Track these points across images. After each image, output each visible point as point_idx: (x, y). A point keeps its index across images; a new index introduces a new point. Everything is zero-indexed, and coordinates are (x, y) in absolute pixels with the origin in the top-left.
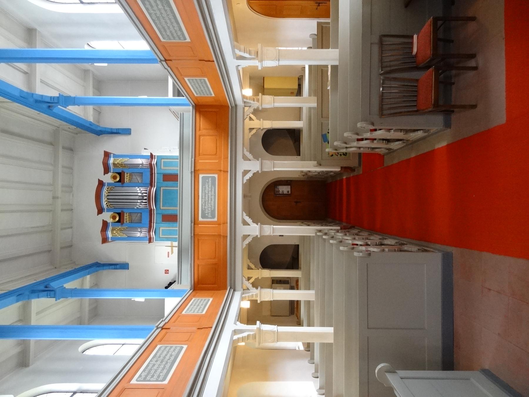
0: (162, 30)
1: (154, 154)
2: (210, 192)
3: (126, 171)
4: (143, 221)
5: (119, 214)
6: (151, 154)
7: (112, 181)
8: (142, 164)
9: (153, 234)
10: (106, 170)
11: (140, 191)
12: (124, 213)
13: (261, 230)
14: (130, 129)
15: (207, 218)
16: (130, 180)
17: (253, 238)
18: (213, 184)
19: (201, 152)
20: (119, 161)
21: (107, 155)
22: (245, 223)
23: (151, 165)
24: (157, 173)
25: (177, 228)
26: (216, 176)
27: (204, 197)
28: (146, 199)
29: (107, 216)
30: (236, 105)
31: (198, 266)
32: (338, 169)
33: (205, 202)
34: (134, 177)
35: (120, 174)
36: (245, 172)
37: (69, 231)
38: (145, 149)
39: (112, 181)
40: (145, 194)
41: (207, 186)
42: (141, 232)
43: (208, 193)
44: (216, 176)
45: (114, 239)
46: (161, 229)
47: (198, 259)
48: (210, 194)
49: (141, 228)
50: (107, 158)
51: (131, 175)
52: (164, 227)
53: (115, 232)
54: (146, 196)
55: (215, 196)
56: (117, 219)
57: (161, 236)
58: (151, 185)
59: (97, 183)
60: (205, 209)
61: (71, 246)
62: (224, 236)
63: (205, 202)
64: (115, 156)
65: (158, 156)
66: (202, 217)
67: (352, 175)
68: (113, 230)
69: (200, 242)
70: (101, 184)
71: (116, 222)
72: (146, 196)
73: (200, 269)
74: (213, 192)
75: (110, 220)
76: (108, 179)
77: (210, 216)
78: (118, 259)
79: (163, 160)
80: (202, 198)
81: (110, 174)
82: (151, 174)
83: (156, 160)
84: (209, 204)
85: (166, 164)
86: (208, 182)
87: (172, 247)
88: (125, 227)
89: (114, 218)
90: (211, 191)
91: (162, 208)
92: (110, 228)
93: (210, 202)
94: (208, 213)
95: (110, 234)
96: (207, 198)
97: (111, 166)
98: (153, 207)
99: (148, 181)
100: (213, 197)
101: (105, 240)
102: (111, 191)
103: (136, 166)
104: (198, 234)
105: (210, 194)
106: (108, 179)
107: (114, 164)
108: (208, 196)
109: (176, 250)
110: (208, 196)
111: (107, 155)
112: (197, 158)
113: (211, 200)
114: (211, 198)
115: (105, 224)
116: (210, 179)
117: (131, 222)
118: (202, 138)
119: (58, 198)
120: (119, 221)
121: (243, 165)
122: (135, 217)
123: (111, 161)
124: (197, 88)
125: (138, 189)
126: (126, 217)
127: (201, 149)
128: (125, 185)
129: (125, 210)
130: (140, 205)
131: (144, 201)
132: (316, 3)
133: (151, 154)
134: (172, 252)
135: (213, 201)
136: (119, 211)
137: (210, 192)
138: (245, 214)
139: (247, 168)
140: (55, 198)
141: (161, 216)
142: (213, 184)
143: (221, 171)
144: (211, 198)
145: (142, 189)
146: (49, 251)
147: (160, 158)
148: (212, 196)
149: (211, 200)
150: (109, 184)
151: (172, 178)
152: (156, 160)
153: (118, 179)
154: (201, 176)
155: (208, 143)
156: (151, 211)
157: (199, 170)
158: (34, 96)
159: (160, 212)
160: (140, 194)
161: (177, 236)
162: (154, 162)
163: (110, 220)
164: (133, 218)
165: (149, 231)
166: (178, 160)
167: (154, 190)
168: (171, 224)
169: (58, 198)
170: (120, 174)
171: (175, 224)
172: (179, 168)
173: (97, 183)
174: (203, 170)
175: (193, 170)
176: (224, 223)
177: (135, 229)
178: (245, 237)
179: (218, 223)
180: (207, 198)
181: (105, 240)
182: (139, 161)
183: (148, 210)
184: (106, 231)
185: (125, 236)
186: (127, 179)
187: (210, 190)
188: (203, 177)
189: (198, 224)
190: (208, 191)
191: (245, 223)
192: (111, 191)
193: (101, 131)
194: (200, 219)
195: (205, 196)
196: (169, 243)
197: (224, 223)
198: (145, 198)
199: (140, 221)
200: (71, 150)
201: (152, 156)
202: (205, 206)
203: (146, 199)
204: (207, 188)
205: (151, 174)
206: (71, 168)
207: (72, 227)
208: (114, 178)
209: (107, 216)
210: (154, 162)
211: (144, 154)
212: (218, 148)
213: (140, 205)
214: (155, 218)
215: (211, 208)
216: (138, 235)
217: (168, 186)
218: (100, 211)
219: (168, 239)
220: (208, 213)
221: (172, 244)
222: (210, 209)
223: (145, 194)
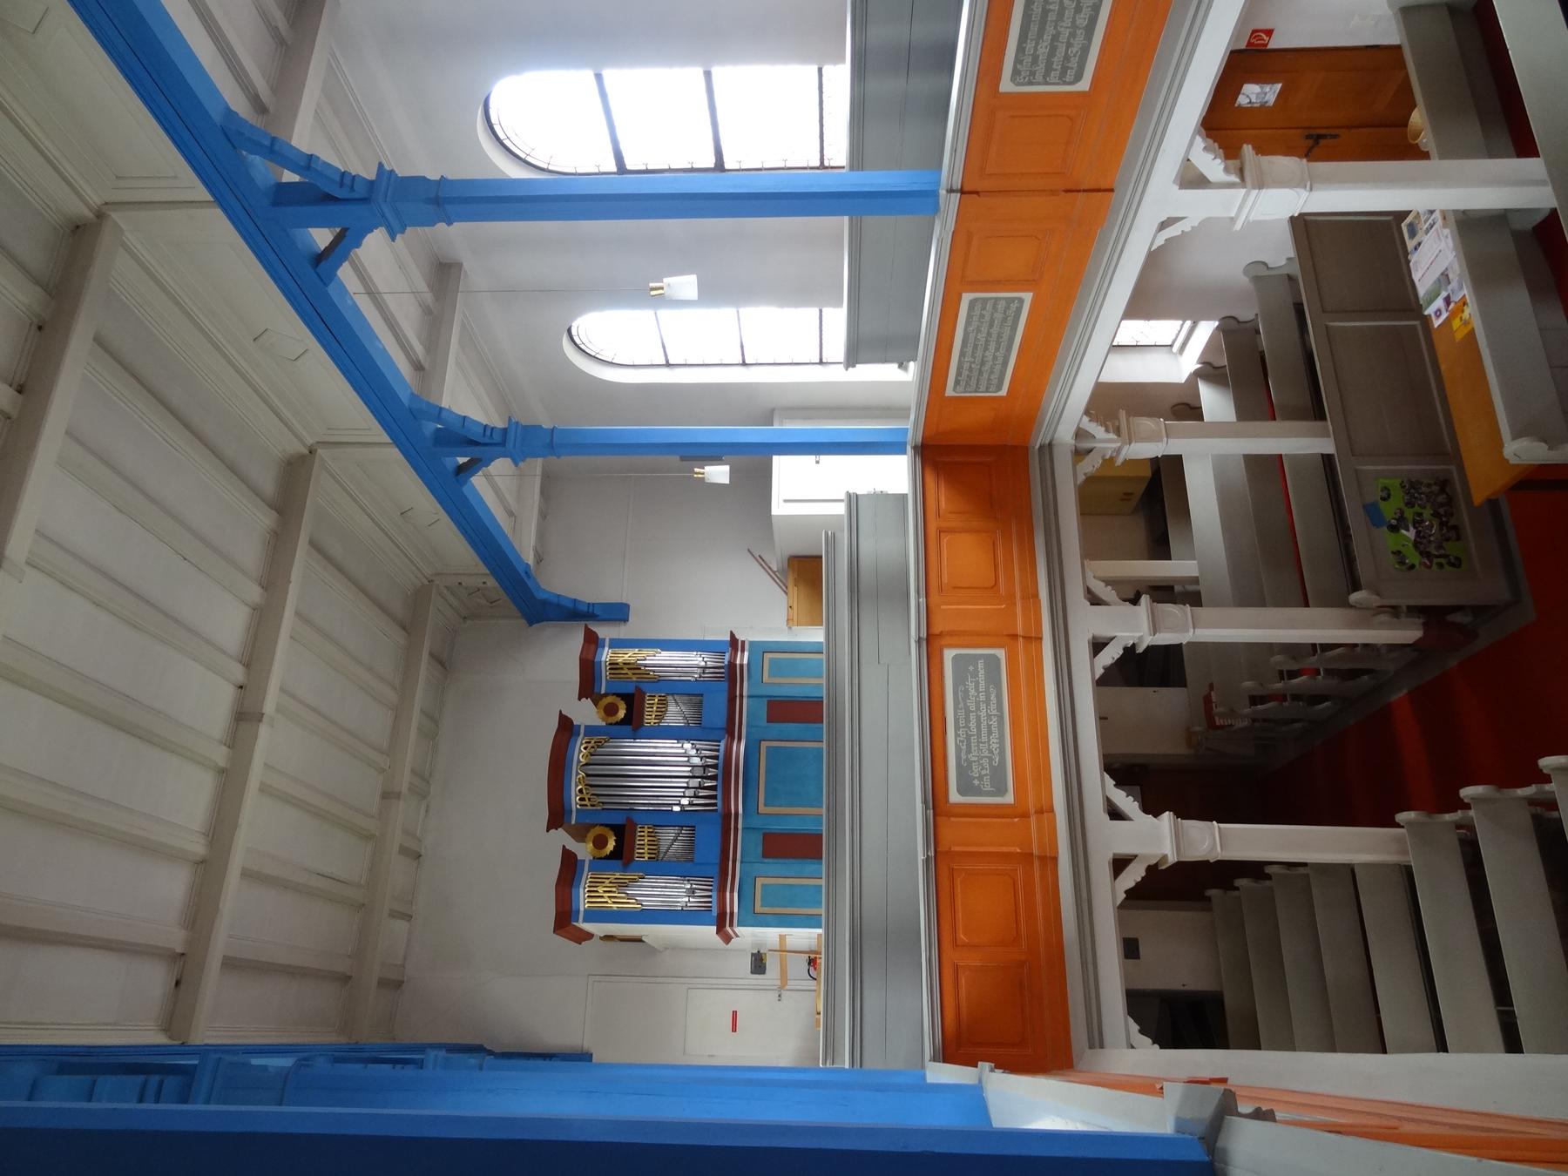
0: (1034, 28)
1: (740, 637)
2: (983, 706)
6: (732, 635)
9: (733, 901)
10: (588, 686)
12: (633, 826)
13: (1178, 836)
14: (627, 606)
15: (979, 793)
17: (1152, 870)
18: (993, 679)
19: (945, 579)
20: (628, 655)
22: (1115, 814)
23: (732, 665)
26: (1001, 653)
27: (962, 723)
28: (714, 778)
30: (1050, 445)
31: (956, 968)
32: (1408, 634)
33: (968, 737)
36: (1098, 646)
37: (400, 926)
41: (971, 686)
42: (692, 892)
43: (978, 708)
44: (1001, 653)
46: (760, 882)
47: (955, 944)
48: (983, 714)
52: (774, 877)
53: (601, 890)
54: (715, 766)
55: (1001, 718)
57: (758, 909)
58: (730, 730)
60: (970, 763)
61: (398, 985)
62: (1042, 859)
63: (968, 737)
65: (752, 643)
66: (961, 791)
67: (1453, 663)
68: (594, 884)
69: (958, 882)
70: (566, 727)
71: (607, 857)
72: (715, 766)
73: (963, 981)
74: (993, 707)
77: (988, 788)
78: (554, 1038)
80: (957, 728)
84: (984, 747)
85: (777, 668)
86: (975, 674)
90: (988, 702)
91: (762, 809)
92: (586, 877)
93: (984, 739)
94: (980, 778)
95: (583, 902)
96: (973, 725)
97: (605, 674)
99: (720, 720)
100: (994, 722)
104: (948, 852)
105: (983, 714)
107: (614, 666)
108: (978, 718)
110: (978, 718)
112: (935, 598)
113: (990, 733)
114: (989, 727)
115: (570, 866)
116: (981, 664)
117: (655, 857)
118: (945, 539)
119: (398, 796)
120: (615, 855)
121: (1087, 622)
123: (606, 655)
124: (975, 347)
125: (688, 746)
127: (945, 571)
131: (708, 784)
132: (1308, 137)
133: (732, 635)
135: (996, 734)
136: (619, 819)
137: (983, 706)
138: (1110, 782)
139: (1103, 632)
140: (388, 795)
142: (993, 679)
143: (1015, 637)
144: (989, 727)
145: (699, 745)
146: (345, 979)
147: (761, 649)
148: (989, 717)
149: (990, 733)
150: (591, 731)
151: (800, 711)
153: (622, 714)
154: (949, 654)
155: (968, 555)
156: (726, 816)
157: (940, 635)
158: (444, 415)
159: (756, 822)
160: (696, 761)
162: (743, 658)
163: (584, 851)
164: (664, 845)
165: (722, 890)
166: (823, 656)
168: (794, 866)
169: (398, 796)
171: (809, 866)
174: (952, 633)
175: (924, 634)
176: (1040, 812)
178: (1120, 864)
179: (1017, 813)
180: (973, 725)
181: (564, 921)
184: (571, 886)
187: (982, 698)
188: (955, 658)
189: (949, 815)
190: (978, 704)
191: (1115, 814)
193: (545, 603)
194: (955, 797)
195: (967, 720)
197: (1040, 812)
198: (712, 772)
200: (442, 663)
201: (734, 643)
202: (969, 751)
203: (714, 778)
204: (972, 692)
206: (435, 722)
207: (408, 917)
208: (610, 710)
210: (743, 658)
212: (1001, 567)
214: (743, 844)
215: (991, 759)
218: (557, 817)
220: (980, 778)
222: (985, 762)
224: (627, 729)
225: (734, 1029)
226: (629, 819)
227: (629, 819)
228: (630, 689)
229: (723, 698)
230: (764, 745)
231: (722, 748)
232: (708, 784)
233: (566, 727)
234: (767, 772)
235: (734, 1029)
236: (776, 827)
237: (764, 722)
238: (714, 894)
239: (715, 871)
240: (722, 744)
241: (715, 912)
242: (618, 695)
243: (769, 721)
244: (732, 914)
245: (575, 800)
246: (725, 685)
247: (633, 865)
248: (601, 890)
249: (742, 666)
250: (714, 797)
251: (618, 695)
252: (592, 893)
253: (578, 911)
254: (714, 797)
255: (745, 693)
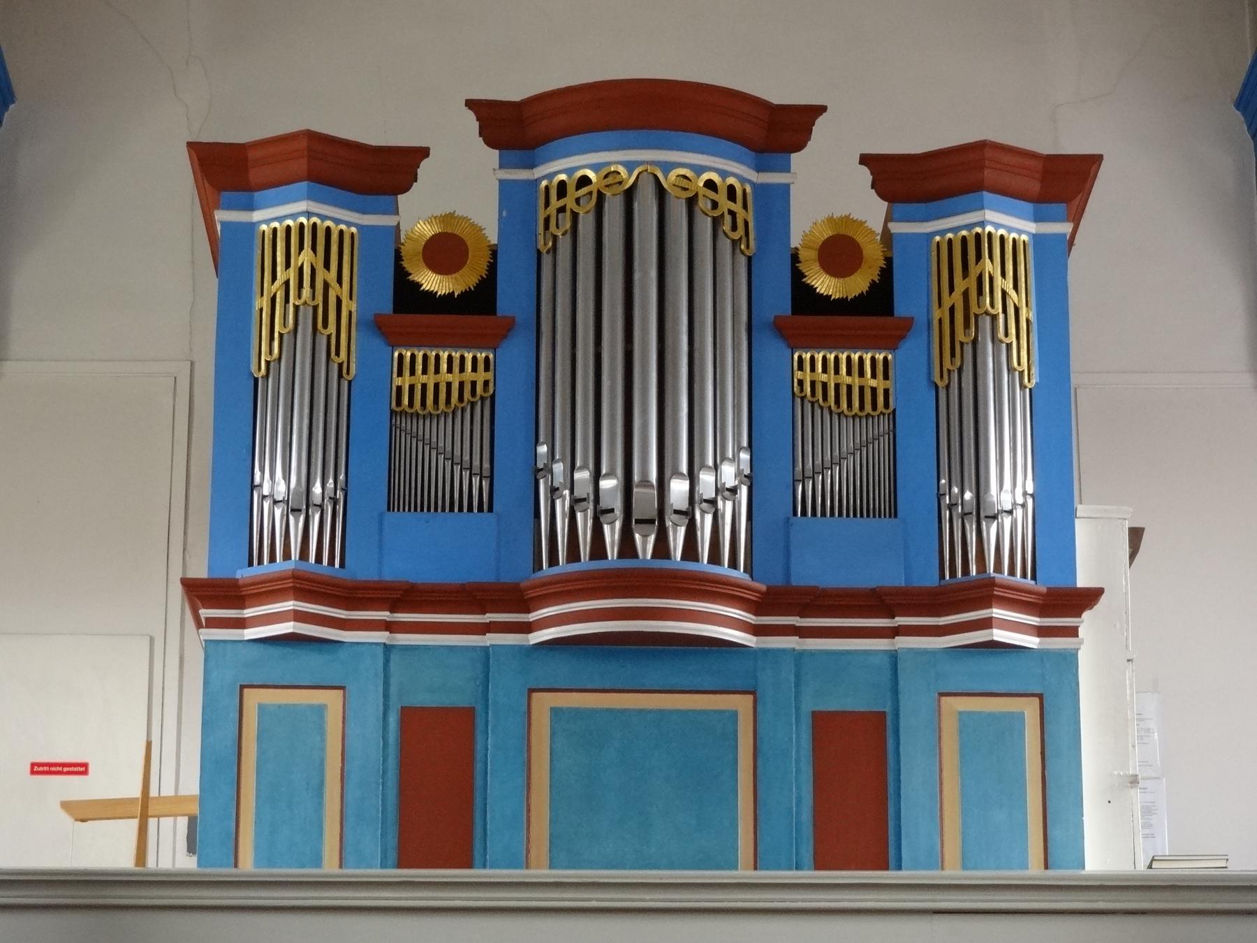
1: (1088, 622)
3: (911, 356)
4: (407, 523)
5: (480, 299)
6: (1091, 597)
7: (805, 224)
8: (981, 513)
9: (276, 619)
11: (716, 484)
12: (492, 340)
16: (818, 399)
20: (1010, 293)
21: (1062, 182)
23: (983, 593)
24: (894, 656)
25: (330, 867)
29: (461, 187)
34: (849, 435)
35: (879, 298)
38: (1136, 535)
39: (805, 224)
40: (677, 539)
42: (300, 505)
45: (230, 254)
46: (332, 700)
49: (342, 504)
50: (1035, 187)
51: (876, 408)
53: (306, 258)
54: (662, 549)
56: (431, 282)
57: (253, 698)
58: (777, 601)
59: (779, 90)
64: (1052, 258)
65: (1069, 661)
68: (324, 242)
70: (779, 130)
71: (401, 275)
72: (662, 549)
75: (416, 216)
76: (827, 190)
79: (1029, 710)
81: (871, 211)
82: (880, 602)
83: (1032, 642)
87: (144, 809)
88: (358, 350)
89: (446, 250)
91: (544, 703)
92: (343, 218)
95: (280, 212)
97: (950, 225)
98: (554, 623)
99: (812, 570)
101: (226, 170)
102: (704, 226)
103: (963, 454)
106: (827, 190)
109: (107, 849)
111: (1062, 182)
115: (382, 172)
120: (408, 296)
122: (447, 447)
123: (1007, 222)
125: (729, 474)
126: (451, 366)
128: (774, 350)
129: (514, 351)
130: (576, 489)
131: (611, 534)
133: (1091, 597)
134: (83, 812)
136: (510, 300)
141: (461, 701)
150: (774, 203)
151: (853, 802)
152: (1032, 642)
153: (824, 284)
156: (515, 598)
159: (505, 688)
160: (678, 488)
161: (248, 864)
163: (416, 216)
164: (440, 433)
165: (303, 586)
166: (1034, 871)
167: (725, 624)
168: (379, 799)
170: (879, 298)
171: (375, 838)
172: (952, 872)
173: (778, 94)
177: (333, 446)
181: (226, 170)
182: (1010, 486)
183: (517, 571)
185: (262, 353)
186: (824, 365)
192: (704, 226)
196: (182, 775)
198: (645, 544)
199: (408, 494)
201: (1067, 602)
205: (880, 602)
208: (840, 251)
209: (461, 187)
210: (1011, 628)
211: (1083, 534)
213: (576, 489)
216: (275, 482)
217: (770, 773)
218: (512, 127)
219: (222, 765)
221: (173, 806)
223: (677, 539)
224: (779, 302)
225: (38, 769)
226: (508, 326)
227: (508, 326)
228: (903, 306)
229: (889, 575)
230: (741, 704)
231: (724, 570)
232: (611, 534)
233: (779, 130)
234: (662, 715)
235: (38, 769)
236: (493, 744)
237: (810, 704)
238: (281, 565)
239: (362, 569)
240: (740, 574)
241: (244, 574)
242: (887, 273)
243: (820, 720)
244: (241, 624)
245: (560, 167)
246: (928, 578)
247: (377, 343)
248: (306, 258)
249: (987, 623)
250: (573, 555)
251: (887, 273)
252: (295, 238)
253: (251, 207)
254: (573, 555)
255: (903, 642)
